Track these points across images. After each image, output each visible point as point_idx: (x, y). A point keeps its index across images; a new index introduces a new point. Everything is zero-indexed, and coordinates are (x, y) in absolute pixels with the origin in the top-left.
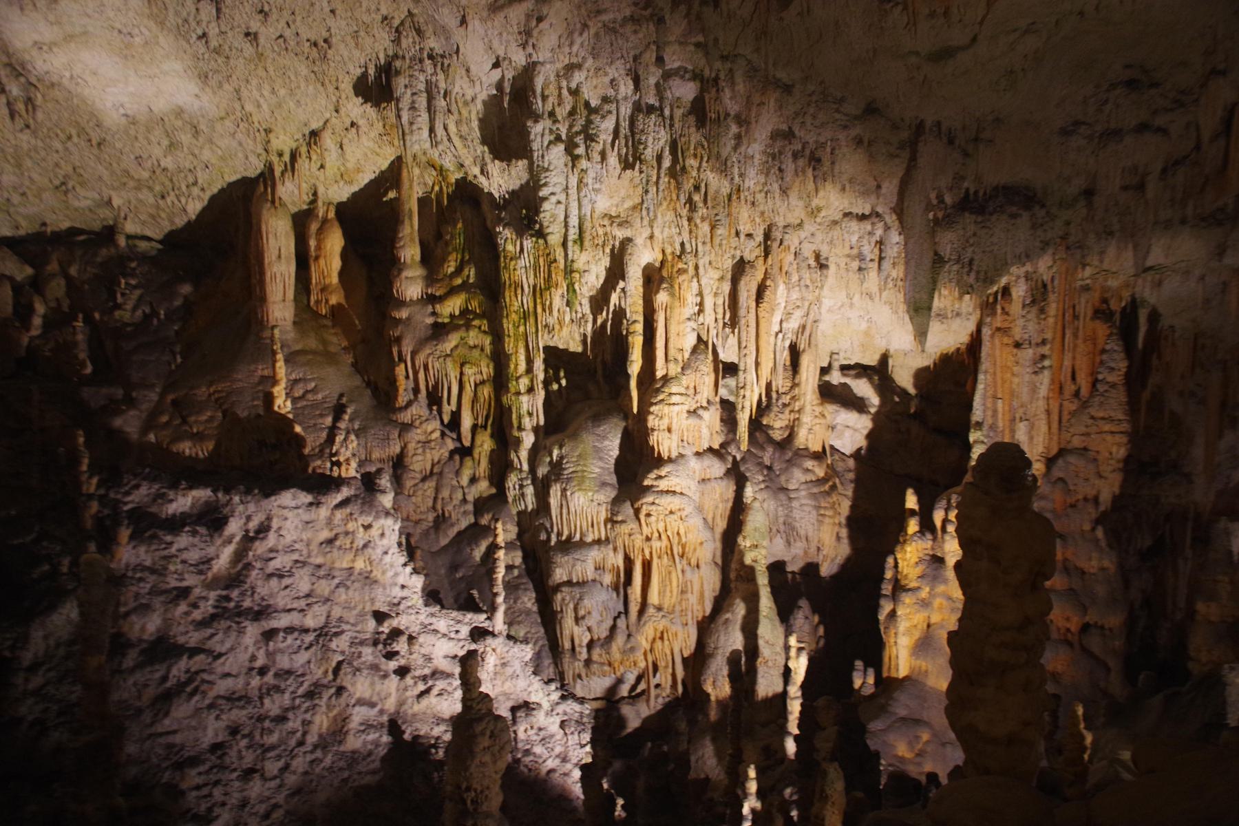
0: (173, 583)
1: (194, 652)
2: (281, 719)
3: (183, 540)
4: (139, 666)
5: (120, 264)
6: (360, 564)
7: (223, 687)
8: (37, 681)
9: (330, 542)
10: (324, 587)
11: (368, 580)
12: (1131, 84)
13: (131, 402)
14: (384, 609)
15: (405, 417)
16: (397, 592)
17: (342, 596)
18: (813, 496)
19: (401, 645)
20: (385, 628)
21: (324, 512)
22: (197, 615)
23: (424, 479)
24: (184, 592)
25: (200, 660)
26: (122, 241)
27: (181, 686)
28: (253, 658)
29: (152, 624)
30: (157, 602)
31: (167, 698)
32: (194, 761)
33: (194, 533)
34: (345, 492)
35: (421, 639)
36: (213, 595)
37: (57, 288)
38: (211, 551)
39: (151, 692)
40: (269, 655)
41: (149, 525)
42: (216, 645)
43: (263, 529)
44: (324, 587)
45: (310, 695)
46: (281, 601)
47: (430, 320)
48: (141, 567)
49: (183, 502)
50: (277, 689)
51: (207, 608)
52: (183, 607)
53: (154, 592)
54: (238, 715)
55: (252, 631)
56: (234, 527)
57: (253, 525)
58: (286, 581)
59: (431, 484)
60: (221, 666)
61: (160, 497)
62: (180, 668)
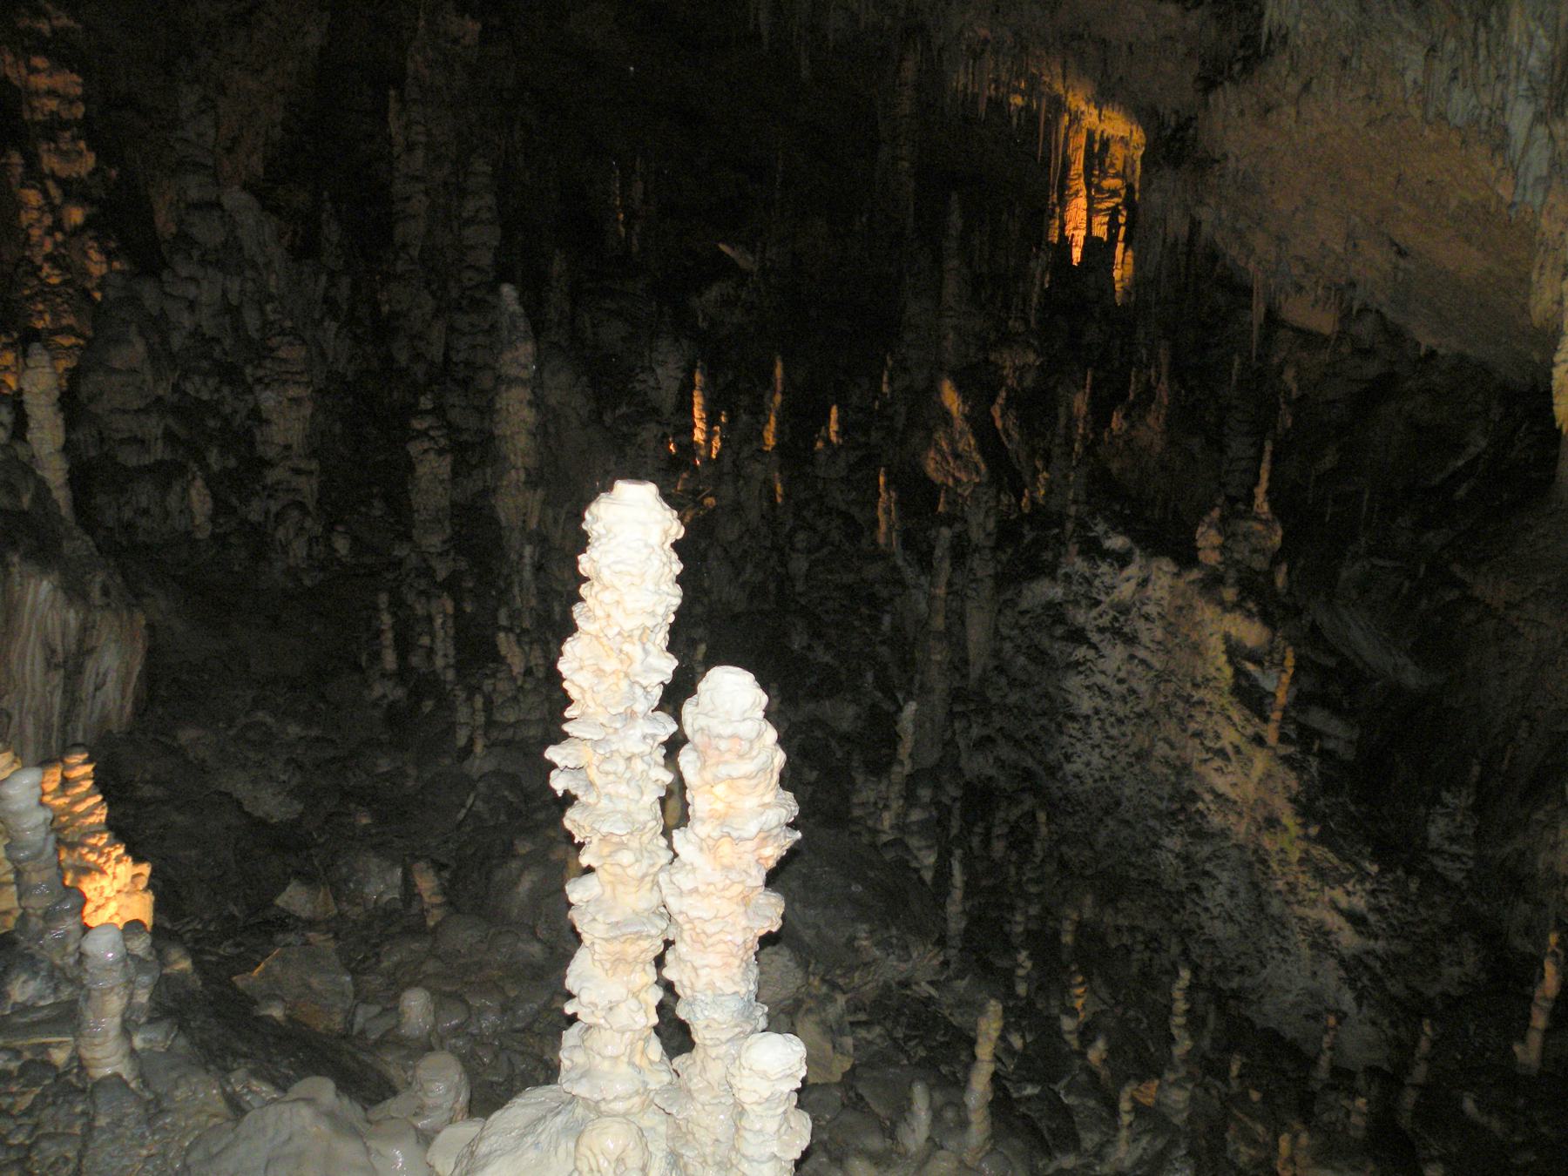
1: (1094, 647)
4: (1063, 638)
8: (1024, 621)
21: (1181, 584)
24: (1097, 603)
25: (1091, 654)
27: (1078, 663)
33: (1111, 565)
36: (1112, 613)
41: (1093, 550)
45: (1139, 716)
46: (1145, 638)
49: (1117, 542)
51: (1105, 621)
52: (1094, 613)
54: (1100, 702)
56: (1132, 570)
62: (1081, 652)
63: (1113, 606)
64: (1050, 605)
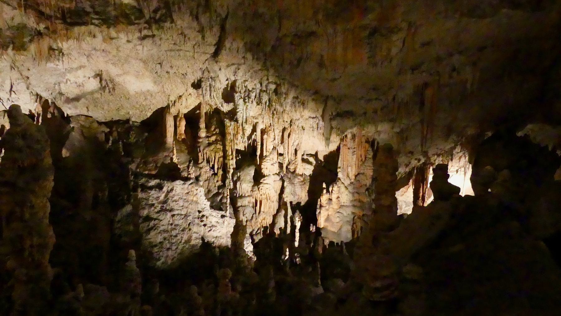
0: (150, 202)
1: (155, 219)
2: (176, 236)
3: (153, 192)
4: (143, 222)
5: (130, 128)
6: (195, 199)
7: (162, 228)
8: (119, 225)
9: (188, 193)
10: (186, 204)
11: (197, 203)
12: (374, 89)
13: (133, 162)
14: (201, 210)
15: (201, 166)
16: (204, 206)
17: (190, 206)
18: (301, 185)
19: (204, 219)
20: (201, 215)
21: (186, 186)
22: (156, 210)
23: (205, 181)
24: (153, 205)
25: (156, 222)
26: (131, 123)
27: (152, 228)
28: (169, 221)
29: (145, 213)
30: (147, 207)
31: (149, 230)
32: (156, 246)
33: (155, 190)
34: (191, 181)
35: (209, 217)
36: (160, 206)
37: (115, 134)
38: (159, 195)
39: (145, 229)
40: (173, 220)
41: (145, 188)
42: (160, 218)
43: (172, 190)
44: (186, 204)
45: (183, 230)
46: (176, 207)
47: (207, 142)
48: (142, 198)
49: (153, 183)
50: (175, 229)
51: (158, 209)
52: (153, 208)
53: (146, 204)
54: (166, 235)
55: (169, 214)
56: (165, 189)
57: (169, 189)
58: (177, 203)
59: (207, 182)
60: (162, 223)
61: (147, 181)
62: (152, 223)
63: (159, 203)
64: (129, 215)
